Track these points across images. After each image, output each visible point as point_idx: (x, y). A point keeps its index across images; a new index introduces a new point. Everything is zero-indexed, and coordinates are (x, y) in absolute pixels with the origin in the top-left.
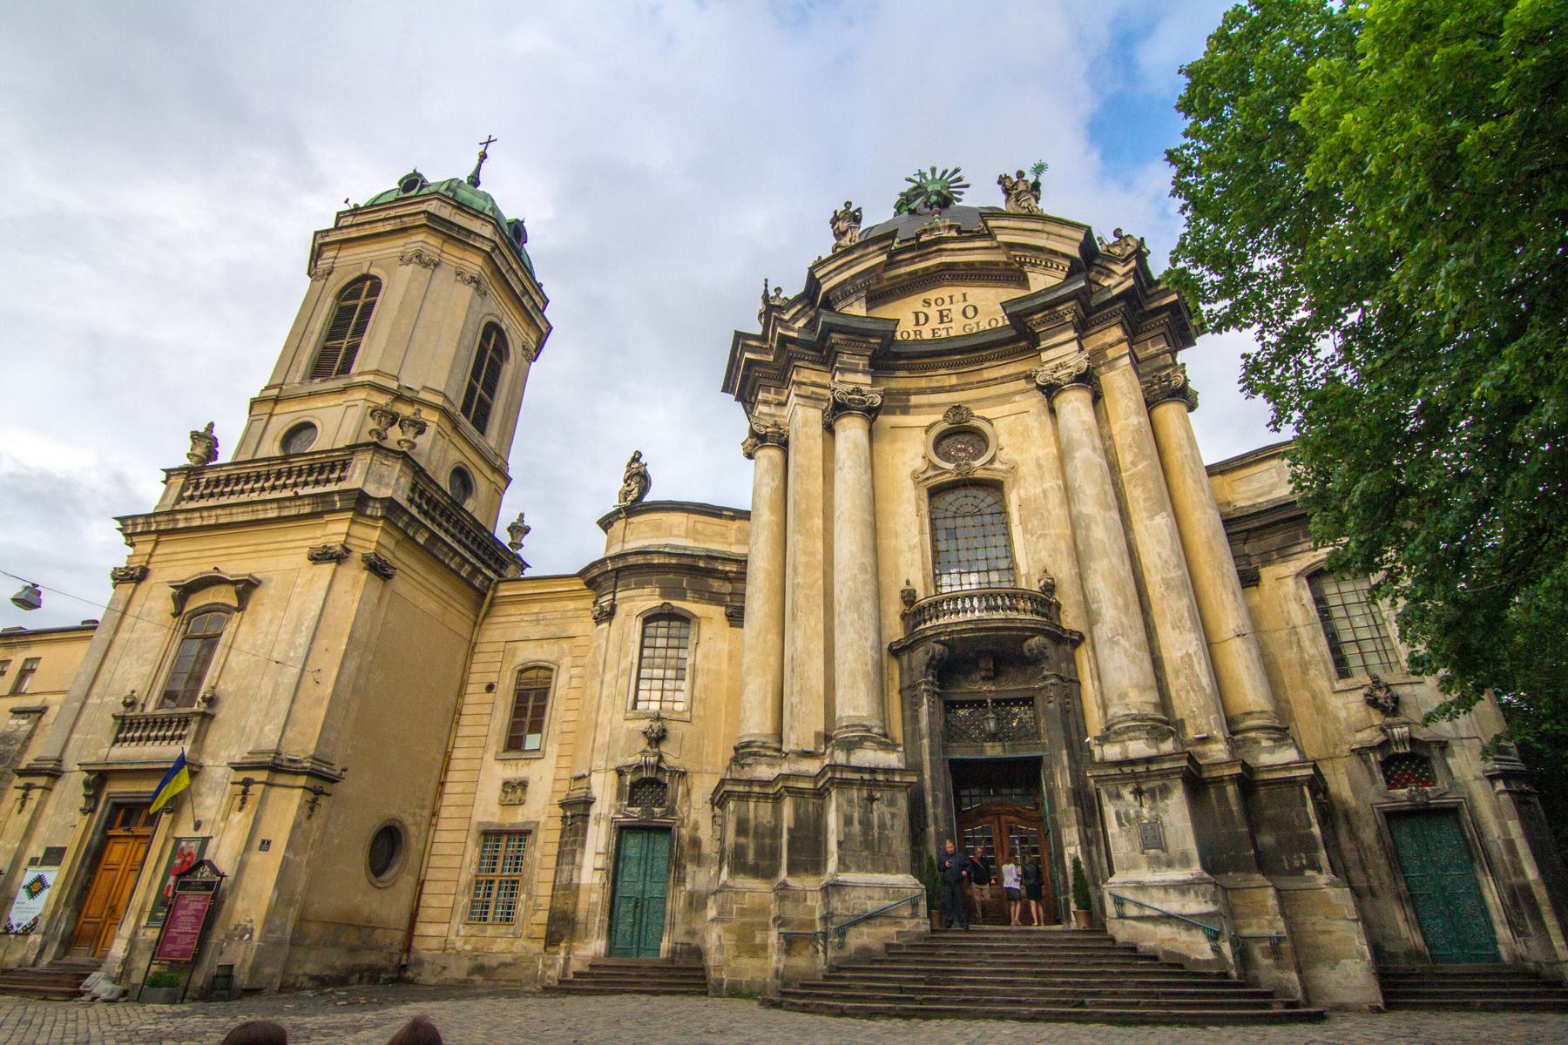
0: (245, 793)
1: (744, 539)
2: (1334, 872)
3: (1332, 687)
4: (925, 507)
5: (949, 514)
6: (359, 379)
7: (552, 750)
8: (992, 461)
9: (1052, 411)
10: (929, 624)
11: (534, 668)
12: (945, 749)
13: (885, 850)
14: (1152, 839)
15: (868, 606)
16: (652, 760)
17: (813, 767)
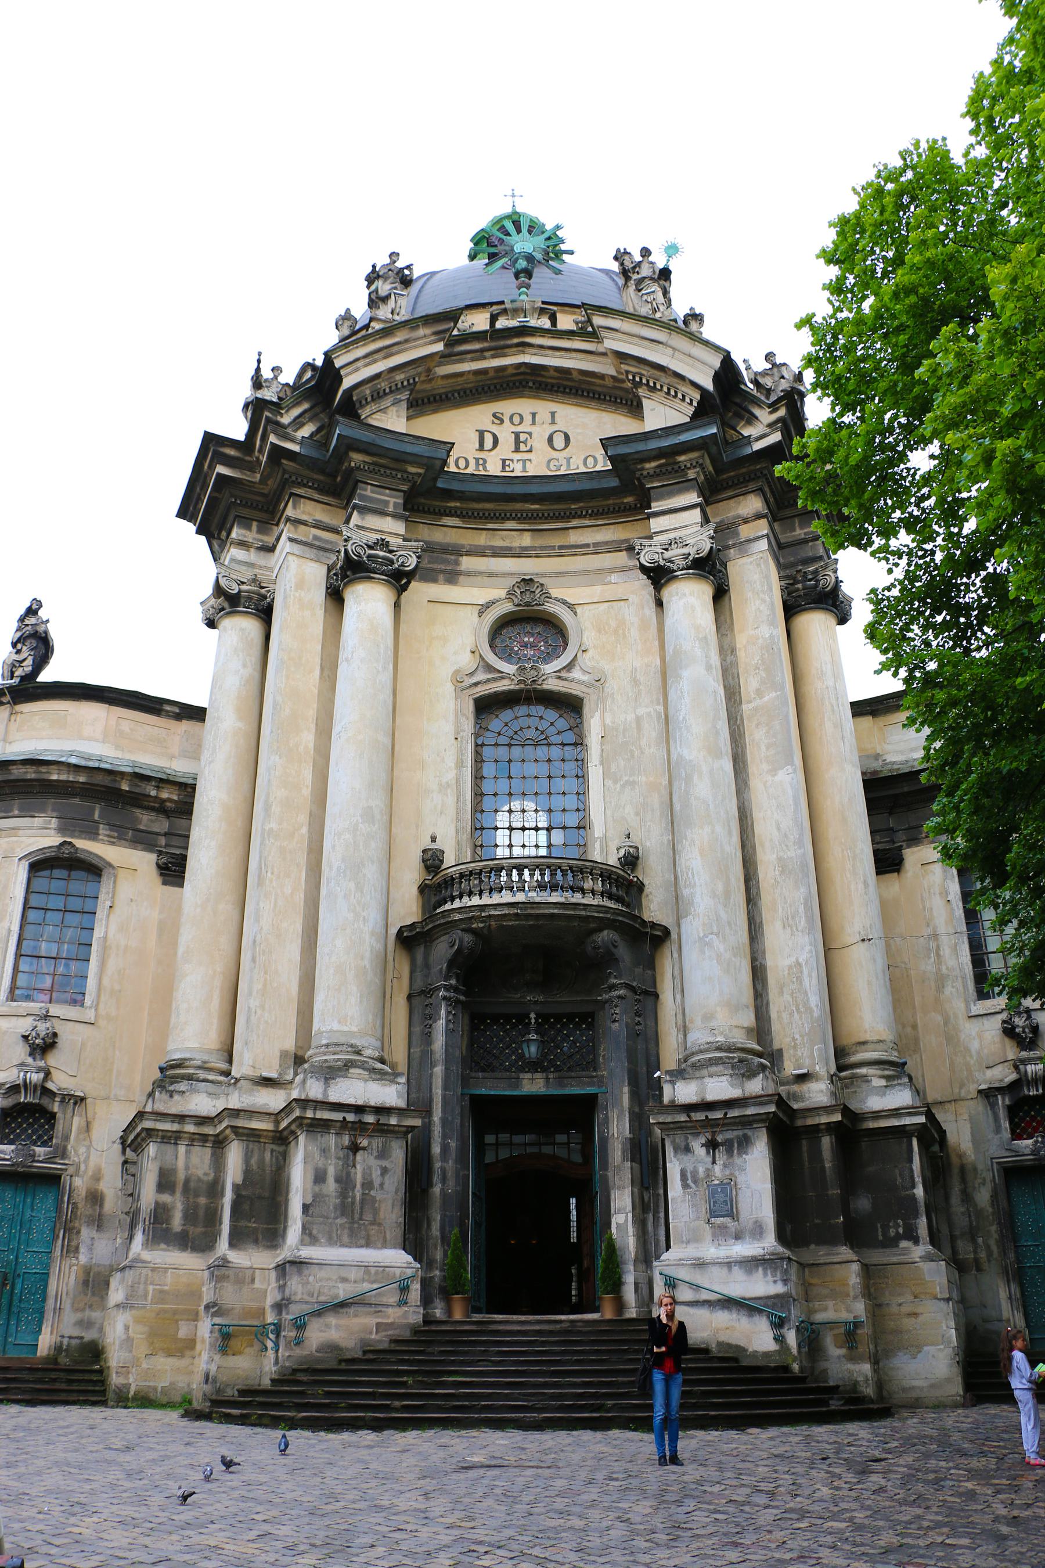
1: (195, 754)
2: (934, 1240)
3: (968, 1009)
4: (468, 725)
5: (503, 740)
8: (569, 667)
9: (659, 603)
10: (457, 904)
12: (465, 1081)
13: (368, 1217)
14: (722, 1206)
15: (372, 872)
16: (36, 1077)
17: (274, 1100)
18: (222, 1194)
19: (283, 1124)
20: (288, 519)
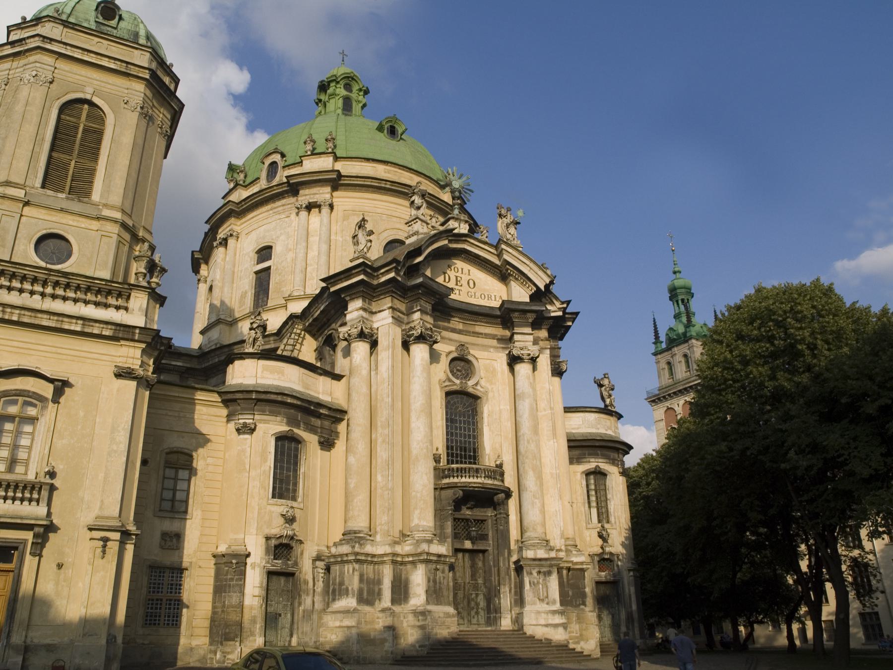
0: (104, 546)
6: (106, 213)
8: (476, 384)
10: (456, 480)
11: (177, 452)
16: (290, 533)
17: (398, 549)
18: (379, 582)
19: (411, 559)
20: (389, 308)
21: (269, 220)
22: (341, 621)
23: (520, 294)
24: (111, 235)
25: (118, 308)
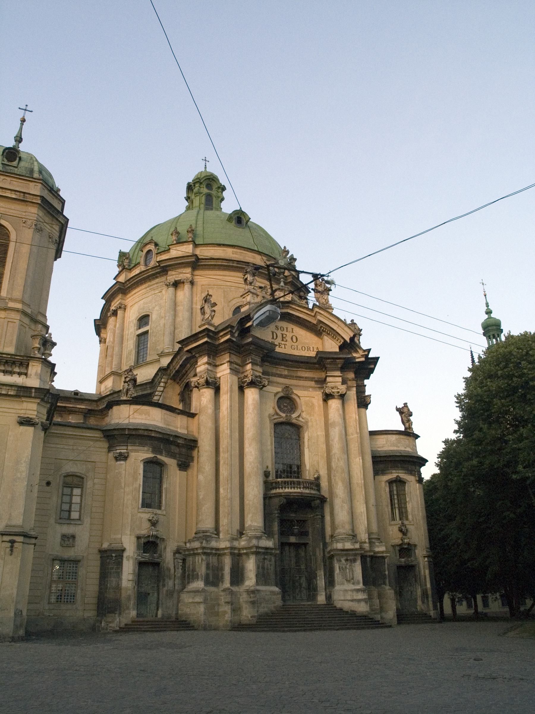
0: (12, 547)
4: (273, 433)
6: (11, 305)
7: (87, 520)
8: (299, 416)
10: (281, 491)
11: (73, 476)
16: (155, 533)
17: (236, 544)
19: (245, 551)
20: (229, 361)
21: (147, 295)
22: (193, 598)
23: (331, 346)
24: (15, 321)
25: (20, 374)
